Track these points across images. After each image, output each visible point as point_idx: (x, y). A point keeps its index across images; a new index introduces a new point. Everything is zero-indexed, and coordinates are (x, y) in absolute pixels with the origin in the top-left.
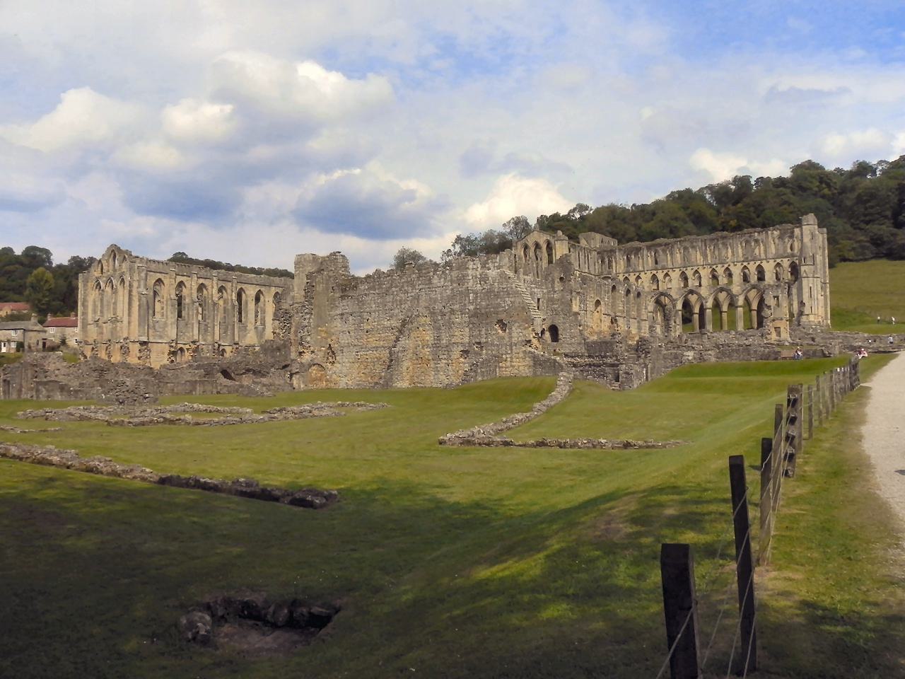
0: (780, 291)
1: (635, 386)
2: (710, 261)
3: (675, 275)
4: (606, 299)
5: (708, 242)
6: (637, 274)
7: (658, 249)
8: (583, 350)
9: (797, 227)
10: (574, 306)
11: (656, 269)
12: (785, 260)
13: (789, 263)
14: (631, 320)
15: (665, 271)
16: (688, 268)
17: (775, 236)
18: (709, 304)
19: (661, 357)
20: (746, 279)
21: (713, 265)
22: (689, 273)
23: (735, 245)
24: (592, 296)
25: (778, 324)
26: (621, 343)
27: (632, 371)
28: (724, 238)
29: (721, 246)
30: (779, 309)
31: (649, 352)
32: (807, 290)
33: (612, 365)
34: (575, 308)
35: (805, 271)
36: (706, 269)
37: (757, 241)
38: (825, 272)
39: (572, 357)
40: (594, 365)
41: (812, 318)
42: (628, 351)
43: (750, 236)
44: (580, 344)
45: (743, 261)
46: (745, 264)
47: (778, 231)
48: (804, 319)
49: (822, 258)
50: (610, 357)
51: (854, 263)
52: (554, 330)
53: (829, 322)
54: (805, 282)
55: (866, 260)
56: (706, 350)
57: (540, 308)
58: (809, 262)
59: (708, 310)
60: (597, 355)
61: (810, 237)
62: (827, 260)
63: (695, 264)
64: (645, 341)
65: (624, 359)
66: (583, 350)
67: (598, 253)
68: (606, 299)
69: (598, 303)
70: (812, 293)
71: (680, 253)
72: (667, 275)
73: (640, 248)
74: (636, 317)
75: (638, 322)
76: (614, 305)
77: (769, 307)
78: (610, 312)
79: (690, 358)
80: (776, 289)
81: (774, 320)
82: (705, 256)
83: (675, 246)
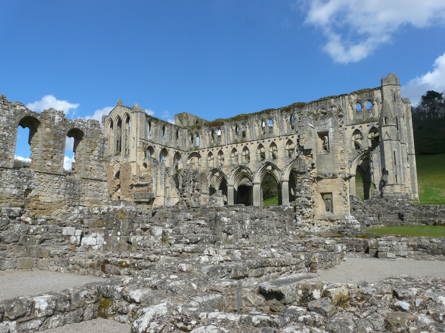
0: (329, 121)
6: (220, 148)
12: (365, 126)
17: (352, 101)
25: (326, 185)
30: (330, 156)
35: (387, 133)
36: (282, 140)
41: (397, 189)
47: (356, 95)
48: (387, 190)
53: (417, 196)
54: (387, 146)
59: (284, 183)
70: (397, 159)
81: (319, 179)
82: (281, 128)
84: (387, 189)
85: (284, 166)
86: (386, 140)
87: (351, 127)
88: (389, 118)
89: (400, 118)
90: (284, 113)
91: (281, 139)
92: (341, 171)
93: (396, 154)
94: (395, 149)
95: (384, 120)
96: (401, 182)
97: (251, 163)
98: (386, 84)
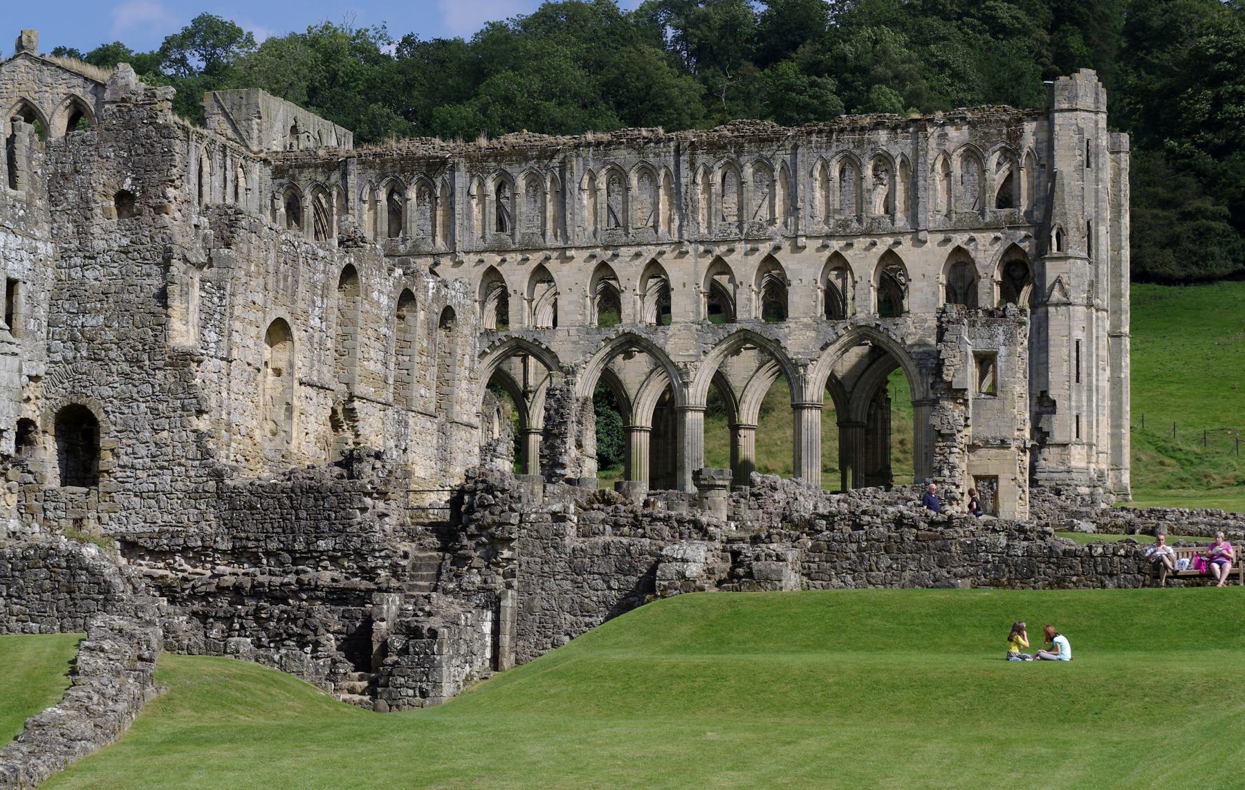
1: (448, 689)
2: (703, 230)
3: (574, 277)
4: (315, 318)
5: (701, 158)
7: (513, 170)
8: (204, 523)
9: (1032, 116)
10: (176, 324)
11: (501, 250)
12: (984, 238)
13: (999, 248)
14: (412, 419)
15: (535, 259)
16: (623, 251)
17: (949, 146)
18: (697, 392)
19: (560, 566)
20: (834, 305)
21: (716, 243)
22: (628, 271)
23: (802, 173)
24: (259, 298)
25: (988, 462)
26: (383, 495)
27: (435, 623)
28: (763, 141)
29: (748, 171)
31: (507, 541)
32: (1065, 351)
33: (337, 596)
34: (183, 331)
36: (690, 259)
37: (883, 162)
38: (1116, 296)
39: (157, 554)
40: (257, 592)
42: (412, 536)
43: (859, 144)
44: (194, 495)
45: (830, 236)
46: (836, 245)
49: (1113, 239)
50: (333, 560)
51: (1191, 289)
52: (78, 432)
53: (1126, 478)
55: (1209, 280)
56: (755, 540)
57: (19, 322)
58: (1075, 245)
60: (273, 545)
61: (1080, 159)
62: (1126, 253)
63: (649, 235)
64: (490, 489)
65: (395, 571)
66: (211, 525)
67: (278, 173)
68: (315, 322)
69: (279, 331)
70: (1083, 364)
71: (594, 191)
72: (541, 275)
73: (444, 161)
74: (432, 408)
75: (442, 431)
76: (345, 353)
77: (957, 394)
78: (327, 377)
79: (693, 570)
80: (988, 325)
83: (577, 165)
84: (1050, 458)
85: (691, 352)
86: (1057, 305)
87: (941, 237)
88: (1071, 233)
89: (1097, 224)
90: (701, 158)
91: (683, 254)
92: (1017, 433)
93: (1083, 349)
94: (1078, 334)
95: (1054, 240)
96: (1090, 435)
97: (561, 333)
98: (1065, 106)
